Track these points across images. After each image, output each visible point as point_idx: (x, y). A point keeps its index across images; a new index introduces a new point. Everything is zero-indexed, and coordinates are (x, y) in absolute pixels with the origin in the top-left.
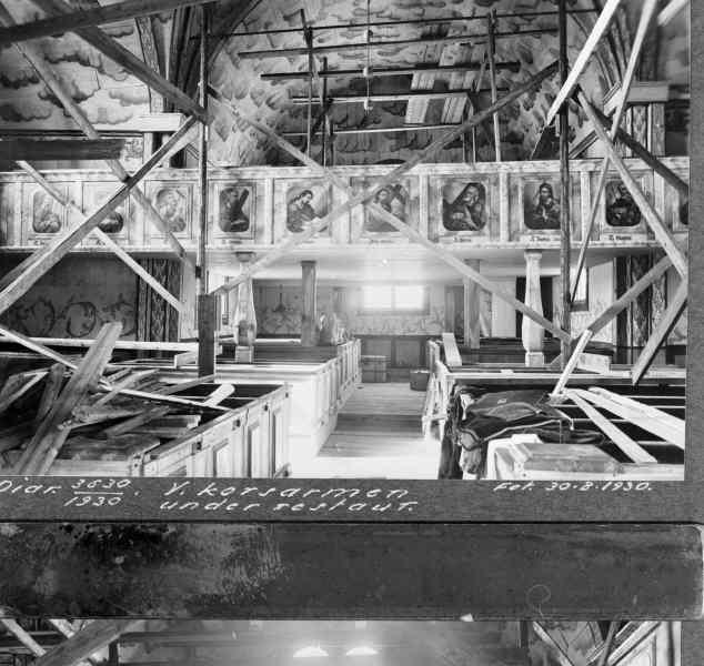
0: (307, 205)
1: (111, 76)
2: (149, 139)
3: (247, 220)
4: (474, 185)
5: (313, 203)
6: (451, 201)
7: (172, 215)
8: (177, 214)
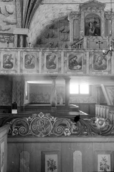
0: (75, 61)
1: (4, 15)
3: (55, 65)
5: (77, 60)
7: (30, 63)
8: (31, 63)
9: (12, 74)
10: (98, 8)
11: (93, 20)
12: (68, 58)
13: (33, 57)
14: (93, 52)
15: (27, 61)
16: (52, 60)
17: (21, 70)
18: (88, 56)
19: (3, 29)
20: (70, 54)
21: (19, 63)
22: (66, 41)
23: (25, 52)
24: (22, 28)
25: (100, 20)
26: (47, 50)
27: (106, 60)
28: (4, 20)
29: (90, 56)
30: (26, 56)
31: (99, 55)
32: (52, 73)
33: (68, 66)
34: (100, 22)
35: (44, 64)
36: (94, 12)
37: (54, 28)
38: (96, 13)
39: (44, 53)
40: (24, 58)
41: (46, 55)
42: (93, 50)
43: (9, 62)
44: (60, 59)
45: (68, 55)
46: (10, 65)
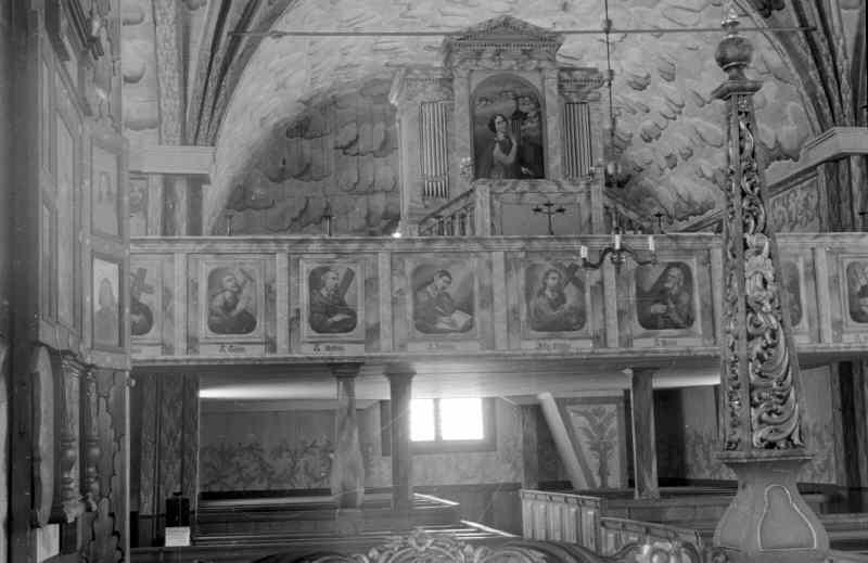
0: (444, 294)
2: (156, 181)
3: (353, 314)
4: (677, 265)
5: (452, 290)
6: (647, 288)
7: (234, 307)
8: (240, 306)
9: (147, 361)
10: (530, 50)
11: (511, 104)
12: (409, 282)
13: (249, 282)
14: (522, 249)
15: (219, 301)
16: (336, 292)
17: (192, 342)
18: (499, 268)
20: (418, 264)
21: (179, 307)
22: (366, 193)
23: (208, 256)
24: (184, 142)
25: (539, 105)
26: (313, 247)
29: (507, 269)
30: (213, 278)
31: (549, 266)
32: (341, 349)
33: (409, 318)
34: (539, 114)
35: (298, 311)
36: (511, 69)
37: (308, 134)
38: (522, 75)
39: (298, 261)
41: (306, 267)
42: (519, 244)
44: (371, 284)
45: (409, 266)
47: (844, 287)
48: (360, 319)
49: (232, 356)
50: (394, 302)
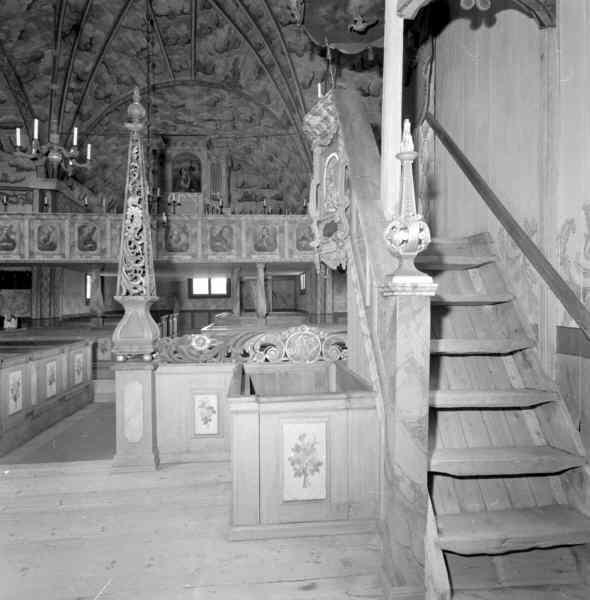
3: (95, 243)
8: (51, 240)
11: (188, 164)
15: (42, 238)
17: (31, 254)
19: (12, 178)
21: (26, 241)
27: (187, 234)
28: (11, 162)
30: (40, 228)
40: (36, 231)
41: (77, 225)
43: (8, 239)
44: (103, 233)
46: (10, 244)
47: (295, 236)
48: (99, 245)
49: (46, 259)
50: (112, 239)
